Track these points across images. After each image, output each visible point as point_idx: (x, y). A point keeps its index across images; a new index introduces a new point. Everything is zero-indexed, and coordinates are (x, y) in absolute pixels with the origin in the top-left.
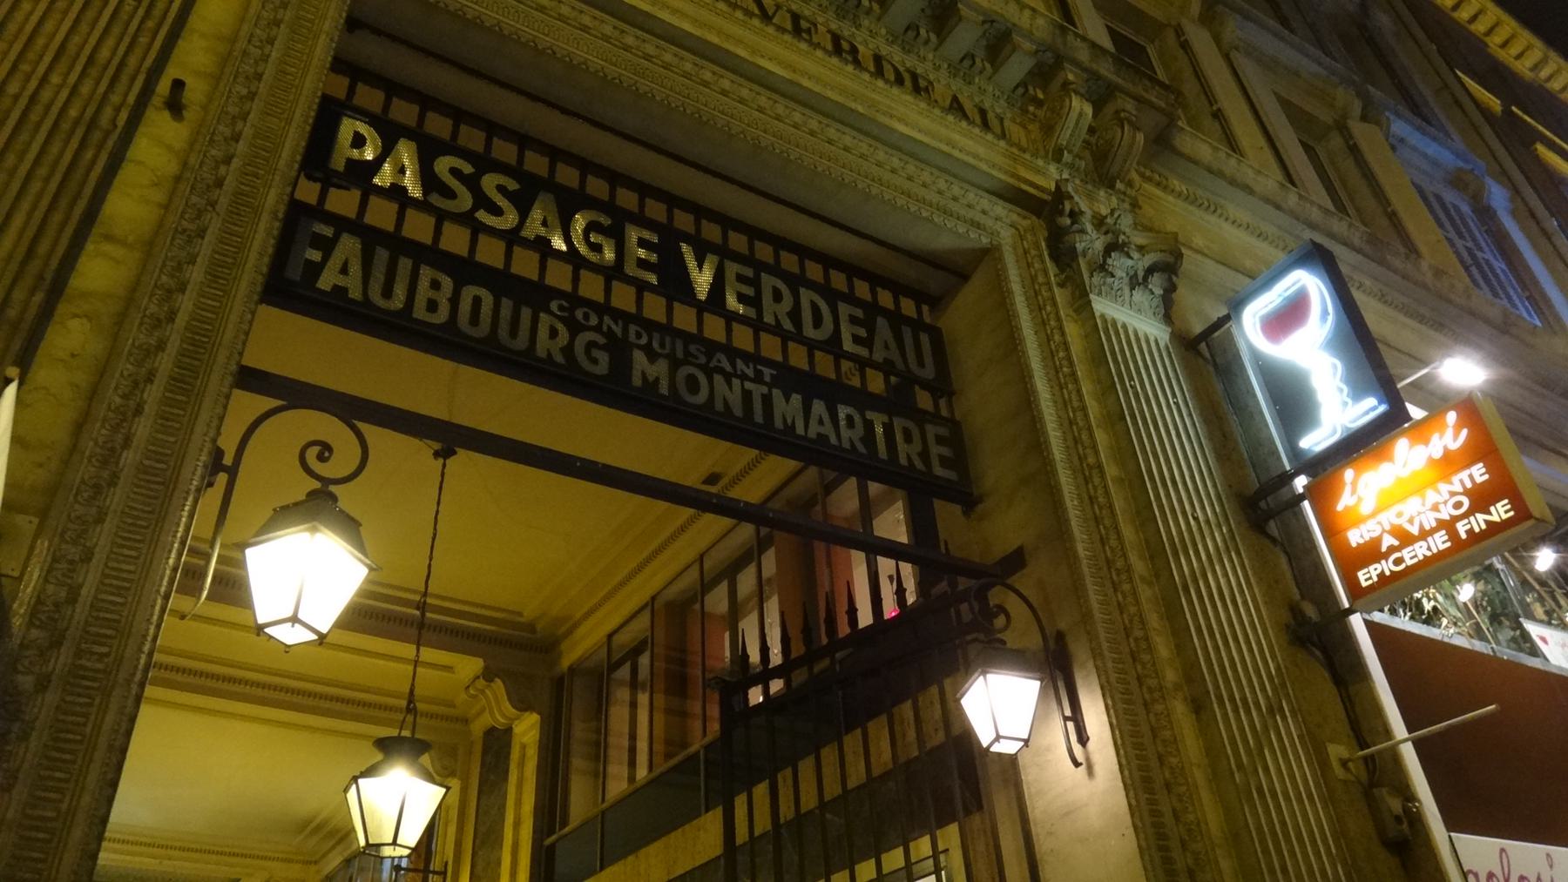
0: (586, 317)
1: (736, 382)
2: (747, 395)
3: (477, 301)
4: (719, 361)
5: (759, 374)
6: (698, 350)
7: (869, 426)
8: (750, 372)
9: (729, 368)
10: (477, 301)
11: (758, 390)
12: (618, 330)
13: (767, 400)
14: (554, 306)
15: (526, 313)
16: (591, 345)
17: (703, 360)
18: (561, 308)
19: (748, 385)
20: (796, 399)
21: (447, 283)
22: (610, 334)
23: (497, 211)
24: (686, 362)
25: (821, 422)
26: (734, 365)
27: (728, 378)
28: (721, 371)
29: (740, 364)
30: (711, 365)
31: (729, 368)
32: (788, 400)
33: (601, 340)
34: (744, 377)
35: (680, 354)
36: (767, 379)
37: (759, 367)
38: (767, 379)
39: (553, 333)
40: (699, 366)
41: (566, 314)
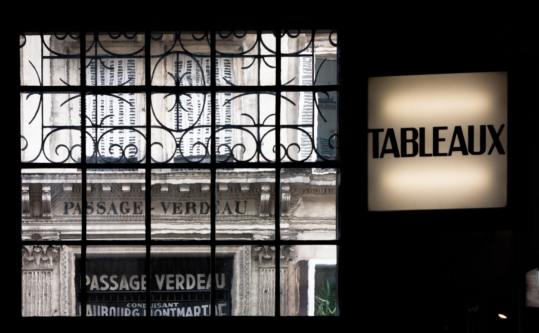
0: (134, 305)
1: (168, 310)
2: (171, 312)
3: (113, 310)
4: (164, 305)
5: (174, 305)
6: (159, 304)
7: (202, 310)
8: (172, 306)
9: (166, 306)
10: (113, 310)
11: (173, 310)
12: (141, 306)
13: (176, 312)
14: (128, 305)
15: (122, 309)
16: (136, 312)
17: (160, 306)
18: (129, 305)
19: (171, 309)
20: (183, 309)
21: (107, 308)
22: (139, 308)
23: (113, 285)
24: (157, 309)
25: (189, 313)
26: (168, 306)
27: (166, 309)
28: (165, 308)
29: (169, 304)
30: (162, 307)
31: (166, 306)
32: (181, 309)
33: (137, 310)
34: (170, 307)
35: (155, 307)
36: (176, 306)
37: (174, 303)
38: (176, 306)
39: (128, 312)
40: (159, 309)
41: (130, 306)
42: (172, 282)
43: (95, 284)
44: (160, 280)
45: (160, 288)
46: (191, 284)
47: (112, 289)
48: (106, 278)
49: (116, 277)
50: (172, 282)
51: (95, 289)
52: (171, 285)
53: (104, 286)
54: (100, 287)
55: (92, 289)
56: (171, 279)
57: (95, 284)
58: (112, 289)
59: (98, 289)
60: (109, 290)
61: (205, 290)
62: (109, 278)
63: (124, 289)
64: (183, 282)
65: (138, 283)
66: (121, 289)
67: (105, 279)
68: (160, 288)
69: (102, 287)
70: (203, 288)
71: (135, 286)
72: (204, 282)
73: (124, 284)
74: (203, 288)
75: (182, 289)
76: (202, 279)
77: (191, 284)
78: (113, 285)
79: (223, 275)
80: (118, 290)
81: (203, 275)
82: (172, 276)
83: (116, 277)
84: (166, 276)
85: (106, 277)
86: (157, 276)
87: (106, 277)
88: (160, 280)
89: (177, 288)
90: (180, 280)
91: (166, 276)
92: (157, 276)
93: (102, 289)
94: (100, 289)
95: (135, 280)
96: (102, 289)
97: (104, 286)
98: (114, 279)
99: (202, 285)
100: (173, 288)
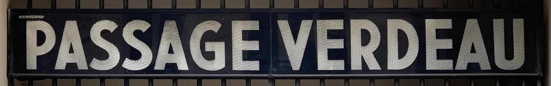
23: (135, 55)
42: (339, 44)
43: (71, 51)
44: (295, 35)
45: (296, 64)
46: (402, 52)
47: (129, 65)
48: (144, 31)
49: (144, 26)
50: (339, 44)
51: (72, 67)
52: (333, 54)
53: (103, 55)
54: (89, 61)
55: (61, 64)
56: (332, 34)
57: (71, 51)
58: (129, 65)
59: (82, 65)
60: (119, 68)
61: (454, 71)
62: (119, 30)
63: (172, 67)
64: (375, 43)
65: (219, 48)
66: (159, 66)
67: (105, 34)
68: (296, 64)
69: (94, 59)
70: (446, 65)
71: (210, 56)
72: (447, 44)
73: (171, 51)
74: (446, 65)
75: (371, 68)
76: (440, 34)
77: (402, 52)
78: (135, 55)
79: (518, 25)
80: (151, 68)
81: (446, 24)
82: (337, 25)
83: (144, 26)
84: (314, 27)
85: (110, 26)
86: (284, 26)
87: (110, 26)
88: (295, 35)
89: (356, 65)
90: (366, 37)
91: (314, 27)
92: (284, 26)
93: (97, 65)
94: (89, 67)
95: (209, 37)
96: (97, 65)
97: (103, 55)
98: (138, 34)
99: (441, 54)
100: (339, 65)
